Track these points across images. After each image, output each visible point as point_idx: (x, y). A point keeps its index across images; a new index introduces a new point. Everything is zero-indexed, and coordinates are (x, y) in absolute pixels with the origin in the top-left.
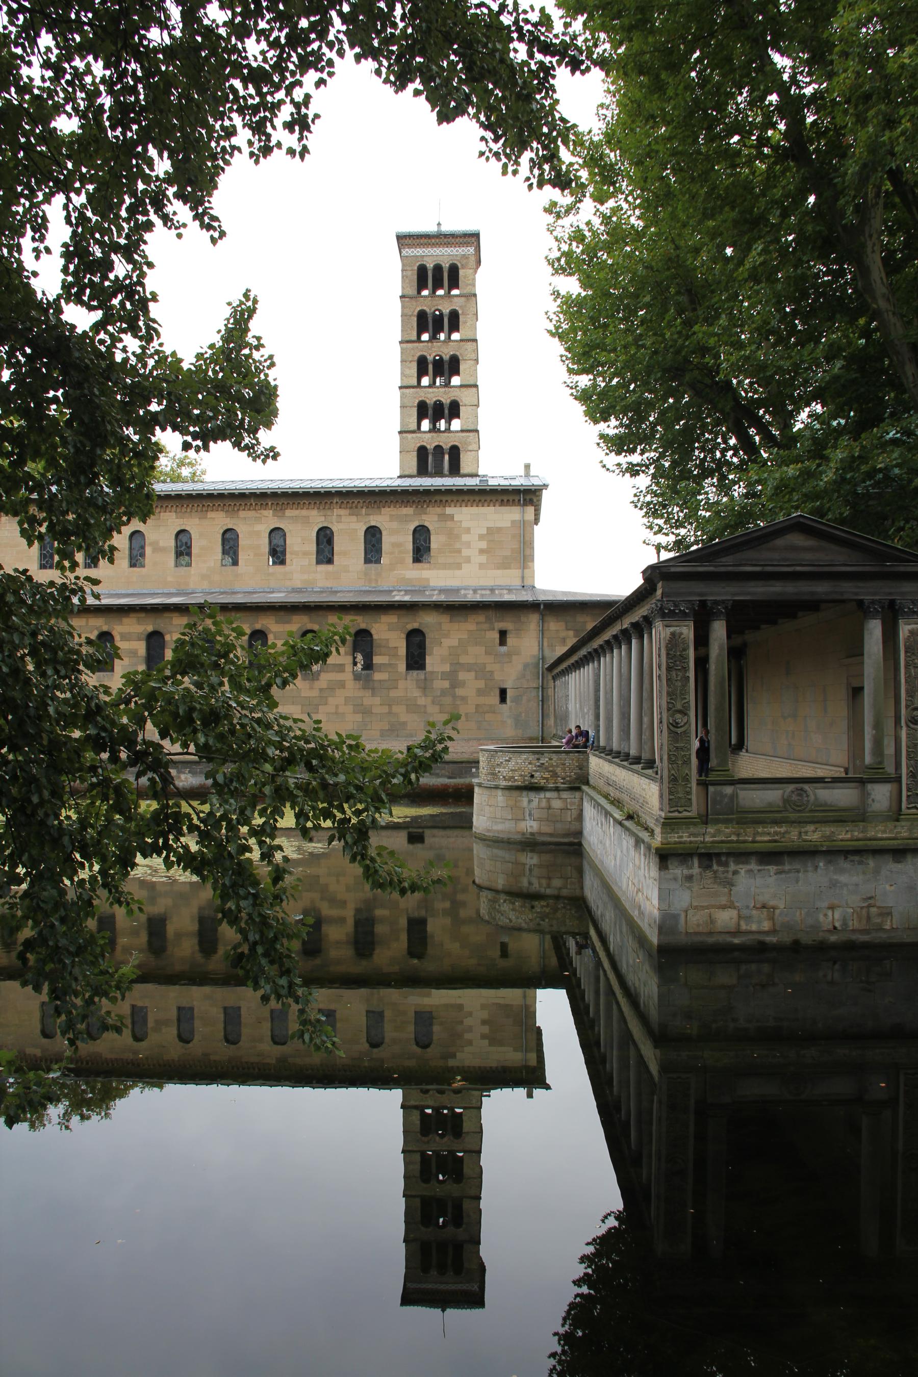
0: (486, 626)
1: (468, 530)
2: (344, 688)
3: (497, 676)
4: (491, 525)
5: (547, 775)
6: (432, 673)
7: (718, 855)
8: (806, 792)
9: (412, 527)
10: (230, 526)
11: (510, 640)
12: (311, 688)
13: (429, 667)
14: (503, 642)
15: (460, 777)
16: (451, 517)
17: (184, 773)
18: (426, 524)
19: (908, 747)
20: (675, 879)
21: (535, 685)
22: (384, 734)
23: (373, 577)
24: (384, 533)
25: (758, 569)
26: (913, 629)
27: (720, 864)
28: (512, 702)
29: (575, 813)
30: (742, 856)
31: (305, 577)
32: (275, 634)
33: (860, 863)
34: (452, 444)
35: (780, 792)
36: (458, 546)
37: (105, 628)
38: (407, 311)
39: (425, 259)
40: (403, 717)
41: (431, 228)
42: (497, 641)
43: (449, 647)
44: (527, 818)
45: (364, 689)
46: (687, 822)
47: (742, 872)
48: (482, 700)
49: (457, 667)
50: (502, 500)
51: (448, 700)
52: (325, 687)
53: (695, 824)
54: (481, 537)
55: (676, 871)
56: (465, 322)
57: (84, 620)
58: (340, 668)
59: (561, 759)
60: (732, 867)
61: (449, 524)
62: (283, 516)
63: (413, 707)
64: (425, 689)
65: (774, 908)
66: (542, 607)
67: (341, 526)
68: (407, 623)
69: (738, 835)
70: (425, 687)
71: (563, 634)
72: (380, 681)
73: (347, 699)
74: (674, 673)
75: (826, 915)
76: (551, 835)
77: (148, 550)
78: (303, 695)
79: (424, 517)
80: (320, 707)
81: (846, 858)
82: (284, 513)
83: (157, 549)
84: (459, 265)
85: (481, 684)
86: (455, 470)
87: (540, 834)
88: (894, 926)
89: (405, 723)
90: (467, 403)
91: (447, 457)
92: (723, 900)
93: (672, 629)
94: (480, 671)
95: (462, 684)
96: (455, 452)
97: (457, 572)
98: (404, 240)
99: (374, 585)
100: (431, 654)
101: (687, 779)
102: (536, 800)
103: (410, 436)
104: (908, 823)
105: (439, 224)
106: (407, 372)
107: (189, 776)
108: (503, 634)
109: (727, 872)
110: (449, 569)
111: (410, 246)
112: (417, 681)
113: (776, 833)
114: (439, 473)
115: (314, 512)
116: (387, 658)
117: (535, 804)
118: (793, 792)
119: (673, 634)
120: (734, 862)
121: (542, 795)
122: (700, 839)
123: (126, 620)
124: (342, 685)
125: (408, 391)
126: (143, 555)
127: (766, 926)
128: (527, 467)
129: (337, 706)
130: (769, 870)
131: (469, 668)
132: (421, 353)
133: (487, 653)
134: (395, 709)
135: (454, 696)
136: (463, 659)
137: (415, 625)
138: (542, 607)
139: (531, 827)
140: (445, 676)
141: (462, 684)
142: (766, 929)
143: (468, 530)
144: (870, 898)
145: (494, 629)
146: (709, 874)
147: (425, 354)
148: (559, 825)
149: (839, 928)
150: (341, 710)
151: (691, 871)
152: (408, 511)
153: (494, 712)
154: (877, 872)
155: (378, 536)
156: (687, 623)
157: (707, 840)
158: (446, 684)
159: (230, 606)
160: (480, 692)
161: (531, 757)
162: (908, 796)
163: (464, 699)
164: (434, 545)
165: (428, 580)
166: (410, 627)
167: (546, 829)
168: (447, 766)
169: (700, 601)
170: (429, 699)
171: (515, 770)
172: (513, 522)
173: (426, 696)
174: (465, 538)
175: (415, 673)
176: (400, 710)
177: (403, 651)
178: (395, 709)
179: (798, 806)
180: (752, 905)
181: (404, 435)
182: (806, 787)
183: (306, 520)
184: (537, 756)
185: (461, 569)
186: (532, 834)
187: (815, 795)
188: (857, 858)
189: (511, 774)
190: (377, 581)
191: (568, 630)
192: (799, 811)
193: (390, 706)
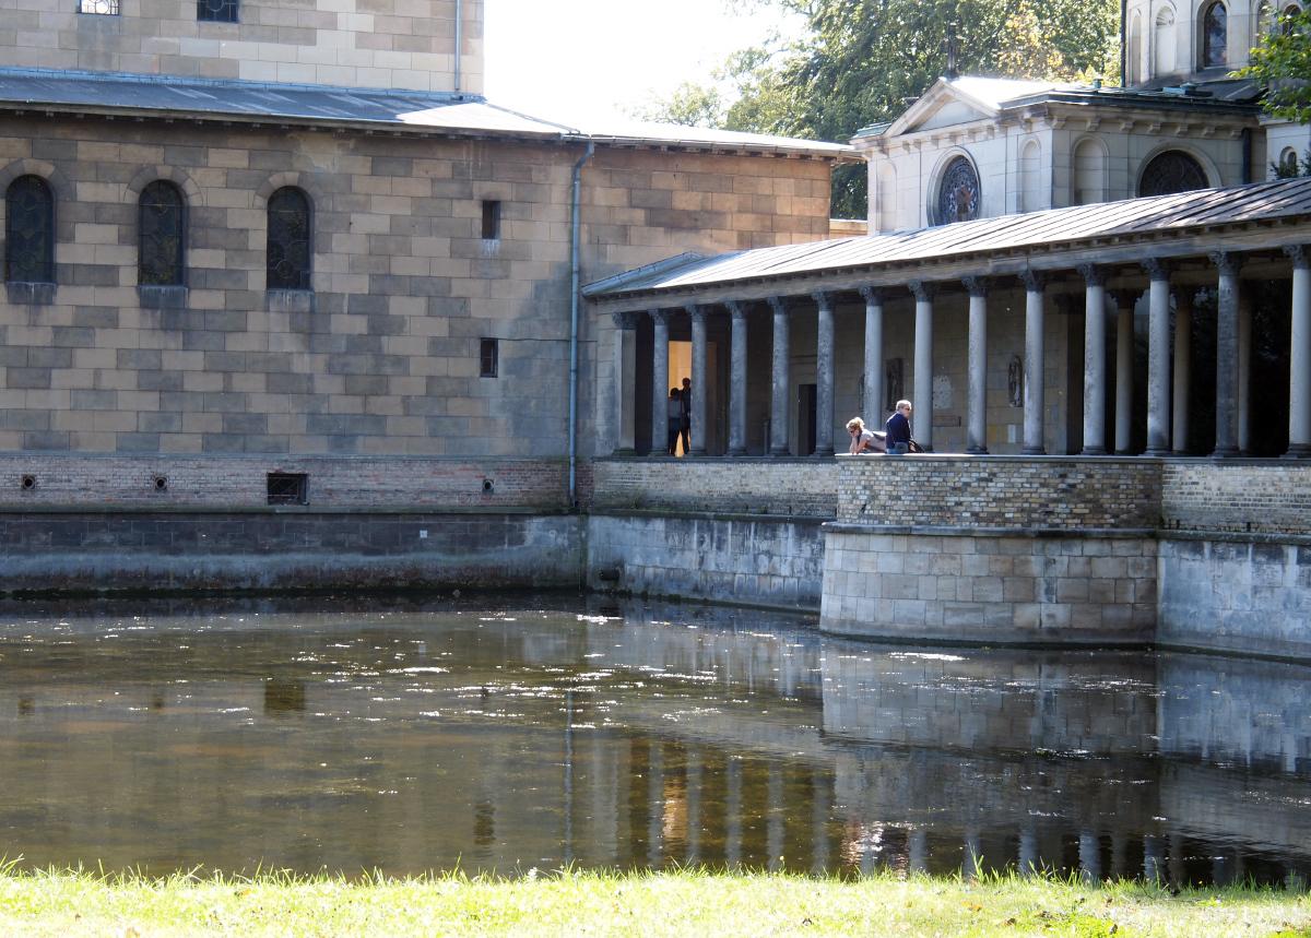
0: (454, 188)
2: (116, 327)
3: (477, 310)
5: (1081, 509)
6: (328, 295)
11: (508, 226)
12: (33, 325)
13: (320, 282)
14: (490, 230)
15: (392, 552)
21: (560, 334)
22: (212, 445)
23: (100, 48)
28: (508, 371)
29: (1142, 586)
40: (261, 403)
42: (478, 226)
43: (369, 235)
44: (1043, 598)
45: (165, 329)
48: (442, 366)
49: (386, 282)
51: (363, 363)
52: (69, 323)
58: (105, 276)
59: (1109, 476)
63: (281, 379)
64: (310, 334)
66: (591, 150)
68: (271, 172)
70: (310, 328)
71: (622, 216)
72: (204, 312)
73: (122, 354)
76: (1094, 632)
78: (11, 342)
80: (55, 373)
85: (440, 328)
87: (1070, 630)
89: (261, 418)
94: (438, 296)
95: (395, 326)
97: (305, 51)
99: (100, 68)
100: (326, 250)
102: (1066, 560)
108: (491, 209)
110: (287, 40)
112: (294, 314)
116: (221, 254)
117: (1060, 568)
121: (1077, 551)
124: (110, 318)
129: (97, 372)
131: (413, 287)
133: (453, 254)
134: (240, 383)
135: (379, 355)
136: (402, 266)
137: (291, 178)
138: (591, 150)
139: (1051, 616)
140: (359, 305)
141: (395, 326)
145: (470, 197)
148: (1110, 613)
150: (106, 383)
153: (468, 396)
158: (360, 325)
160: (438, 347)
161: (1046, 473)
163: (400, 361)
165: (234, 64)
166: (277, 181)
167: (1086, 621)
168: (362, 524)
170: (321, 360)
171: (1007, 500)
173: (312, 352)
175: (287, 296)
176: (250, 383)
177: (259, 240)
178: (240, 383)
184: (1060, 470)
185: (311, 41)
186: (1052, 631)
189: (993, 508)
190: (108, 57)
191: (632, 206)
193: (227, 373)
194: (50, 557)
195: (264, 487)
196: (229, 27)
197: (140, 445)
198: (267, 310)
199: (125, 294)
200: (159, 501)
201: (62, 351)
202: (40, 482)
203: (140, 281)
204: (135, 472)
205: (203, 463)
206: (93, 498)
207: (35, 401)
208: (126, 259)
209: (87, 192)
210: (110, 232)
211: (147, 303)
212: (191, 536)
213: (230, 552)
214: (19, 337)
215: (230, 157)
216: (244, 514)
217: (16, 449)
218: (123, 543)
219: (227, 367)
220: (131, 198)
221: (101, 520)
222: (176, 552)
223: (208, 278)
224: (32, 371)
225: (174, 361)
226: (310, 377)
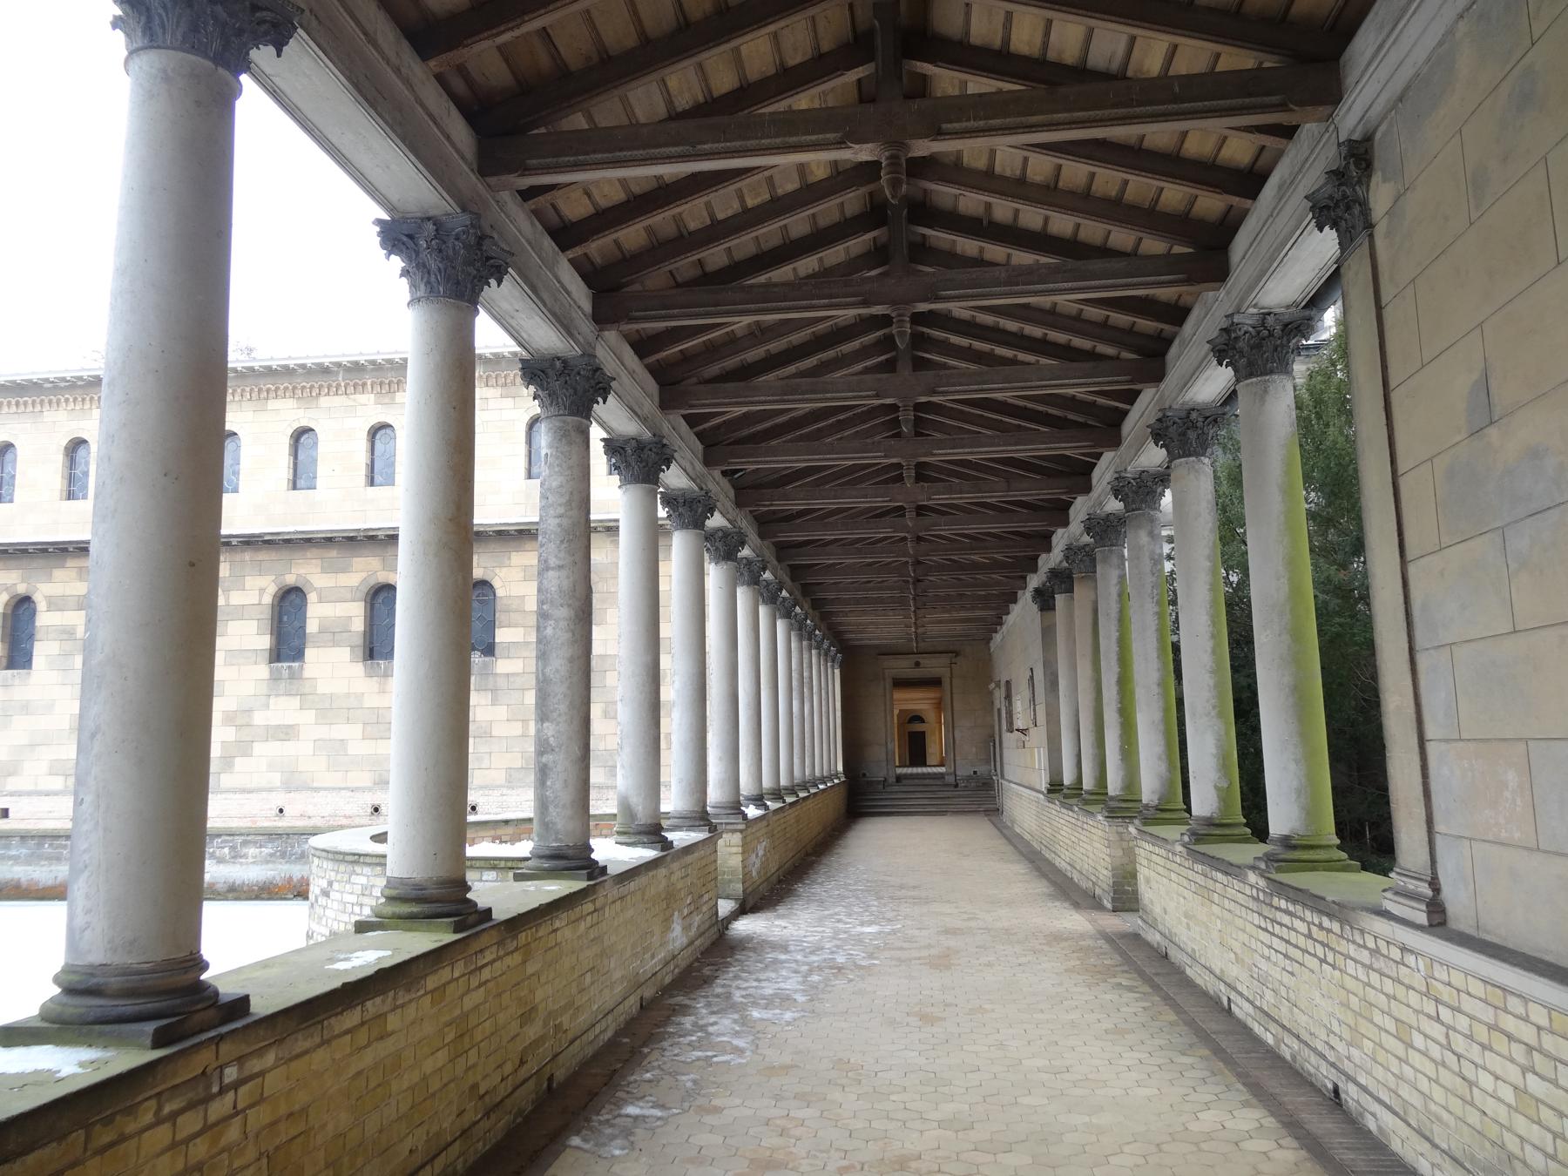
10: (304, 423)
12: (383, 691)
32: (320, 591)
37: (22, 589)
62: (392, 402)
78: (367, 705)
82: (393, 399)
123: (58, 574)
205: (505, 792)
214: (372, 701)
217: (370, 785)
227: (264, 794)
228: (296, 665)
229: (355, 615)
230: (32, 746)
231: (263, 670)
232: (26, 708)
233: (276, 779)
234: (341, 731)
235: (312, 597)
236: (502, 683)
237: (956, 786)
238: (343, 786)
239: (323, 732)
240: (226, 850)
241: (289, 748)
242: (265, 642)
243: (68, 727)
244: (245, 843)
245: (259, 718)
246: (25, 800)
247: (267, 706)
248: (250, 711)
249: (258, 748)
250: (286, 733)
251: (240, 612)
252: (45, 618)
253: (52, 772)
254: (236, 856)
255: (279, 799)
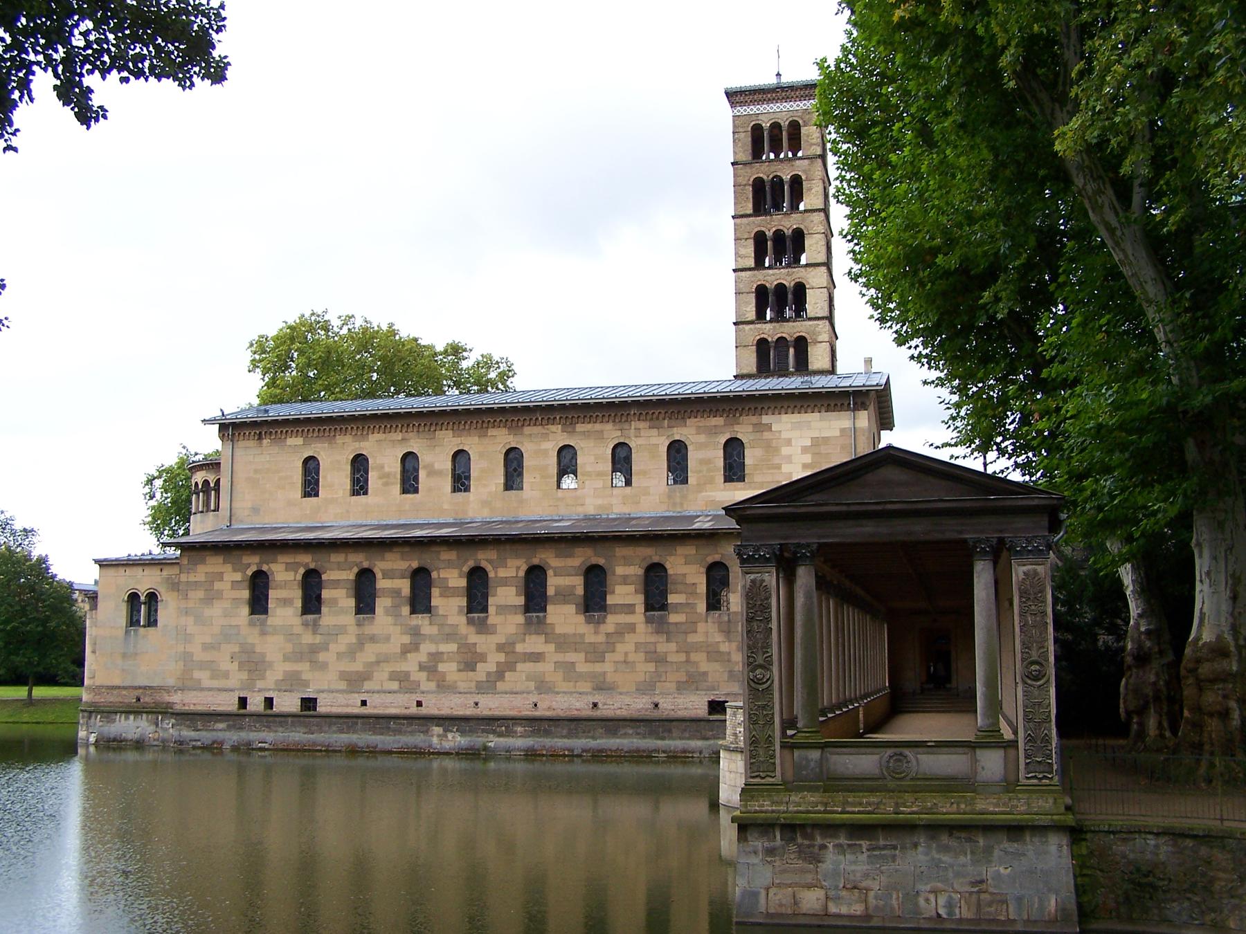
1: (789, 442)
2: (635, 632)
4: (816, 435)
7: (802, 826)
8: (906, 757)
9: (723, 440)
10: (513, 445)
16: (769, 427)
17: (452, 731)
18: (739, 436)
19: (1025, 706)
20: (755, 853)
22: (681, 687)
24: (690, 448)
25: (844, 508)
26: (1029, 571)
27: (805, 836)
30: (830, 828)
31: (600, 502)
32: (555, 569)
33: (969, 840)
34: (798, 334)
35: (876, 757)
36: (776, 461)
37: (366, 565)
38: (741, 180)
39: (760, 117)
40: (704, 667)
41: (769, 80)
45: (657, 633)
46: (771, 789)
47: (830, 846)
50: (829, 405)
53: (778, 791)
54: (805, 450)
55: (756, 843)
56: (809, 189)
57: (343, 555)
58: (630, 608)
60: (819, 840)
61: (766, 435)
62: (574, 431)
64: (729, 632)
65: (868, 890)
67: (640, 441)
68: (707, 555)
69: (826, 804)
72: (676, 624)
74: (755, 624)
75: (927, 900)
77: (422, 474)
79: (737, 428)
81: (951, 835)
82: (574, 428)
83: (432, 473)
84: (801, 122)
86: (802, 365)
88: (1011, 917)
89: (705, 674)
90: (814, 285)
91: (792, 351)
92: (809, 878)
93: (752, 576)
96: (801, 344)
98: (735, 96)
101: (769, 741)
103: (747, 327)
104: (1026, 796)
105: (778, 75)
106: (743, 251)
107: (457, 734)
109: (813, 846)
111: (742, 104)
112: (720, 623)
113: (869, 804)
114: (783, 372)
115: (608, 427)
116: (684, 596)
118: (891, 757)
119: (753, 581)
120: (821, 835)
122: (783, 808)
123: (388, 555)
124: (632, 628)
125: (743, 274)
126: (416, 479)
127: (858, 909)
128: (869, 362)
129: (626, 654)
130: (860, 845)
132: (759, 229)
134: (694, 657)
137: (717, 558)
142: (858, 913)
143: (789, 442)
144: (982, 882)
146: (793, 848)
147: (763, 229)
149: (945, 916)
150: (631, 658)
151: (772, 844)
152: (719, 421)
154: (988, 850)
155: (683, 451)
156: (769, 569)
157: (790, 809)
159: (503, 538)
162: (1027, 764)
164: (748, 461)
166: (710, 560)
169: (780, 544)
172: (843, 430)
173: (730, 641)
174: (785, 451)
176: (699, 657)
177: (702, 588)
178: (694, 657)
179: (897, 773)
180: (841, 885)
181: (741, 327)
182: (907, 752)
183: (600, 436)
187: (917, 760)
188: (963, 835)
190: (682, 504)
192: (899, 779)
193: (687, 653)
194: (604, 741)
195: (706, 707)
196: (740, 485)
197: (646, 687)
198: (707, 622)
199: (639, 617)
200: (656, 714)
201: (610, 646)
202: (600, 705)
203: (647, 610)
204: (644, 700)
205: (676, 696)
206: (623, 713)
207: (598, 668)
208: (639, 600)
209: (620, 570)
210: (631, 588)
211: (649, 621)
212: (670, 731)
213: (689, 739)
214: (591, 638)
215: (689, 550)
216: (696, 720)
217: (590, 690)
218: (638, 734)
219: (687, 650)
220: (641, 572)
221: (628, 723)
222: (663, 739)
223: (678, 608)
224: (596, 654)
225: (662, 648)
226: (729, 653)
227: (525, 695)
228: (541, 614)
229: (577, 584)
230: (378, 662)
231: (520, 619)
232: (373, 639)
233: (532, 685)
234: (571, 657)
235: (550, 573)
236: (672, 628)
237: (958, 695)
238: (574, 690)
239: (560, 657)
240: (503, 728)
241: (539, 667)
242: (521, 601)
243: (399, 651)
244: (516, 724)
245: (519, 648)
246: (376, 695)
247: (524, 641)
248: (514, 643)
249: (520, 666)
250: (537, 657)
251: (505, 582)
252: (382, 583)
253: (391, 679)
254: (509, 733)
255: (534, 698)
